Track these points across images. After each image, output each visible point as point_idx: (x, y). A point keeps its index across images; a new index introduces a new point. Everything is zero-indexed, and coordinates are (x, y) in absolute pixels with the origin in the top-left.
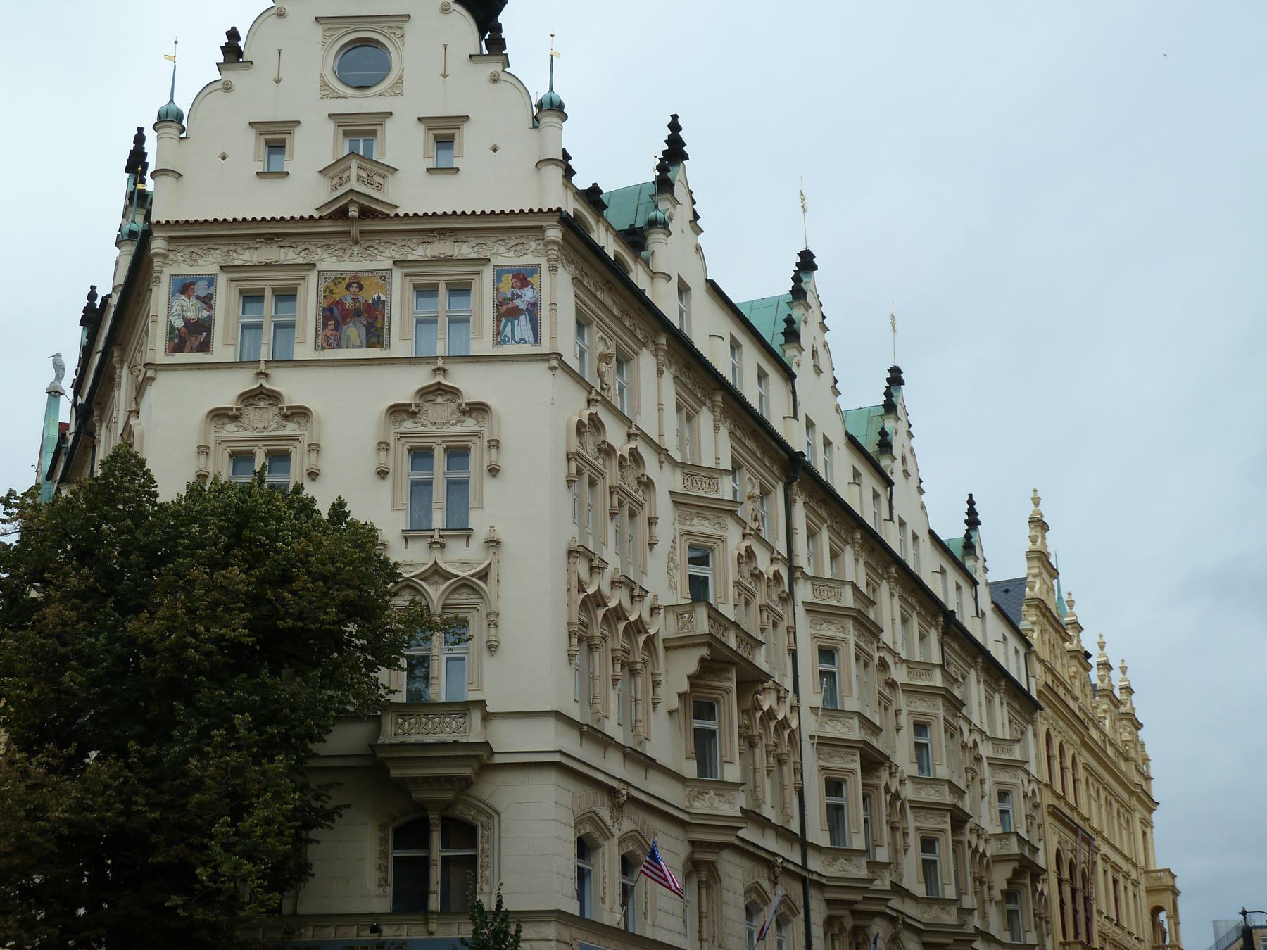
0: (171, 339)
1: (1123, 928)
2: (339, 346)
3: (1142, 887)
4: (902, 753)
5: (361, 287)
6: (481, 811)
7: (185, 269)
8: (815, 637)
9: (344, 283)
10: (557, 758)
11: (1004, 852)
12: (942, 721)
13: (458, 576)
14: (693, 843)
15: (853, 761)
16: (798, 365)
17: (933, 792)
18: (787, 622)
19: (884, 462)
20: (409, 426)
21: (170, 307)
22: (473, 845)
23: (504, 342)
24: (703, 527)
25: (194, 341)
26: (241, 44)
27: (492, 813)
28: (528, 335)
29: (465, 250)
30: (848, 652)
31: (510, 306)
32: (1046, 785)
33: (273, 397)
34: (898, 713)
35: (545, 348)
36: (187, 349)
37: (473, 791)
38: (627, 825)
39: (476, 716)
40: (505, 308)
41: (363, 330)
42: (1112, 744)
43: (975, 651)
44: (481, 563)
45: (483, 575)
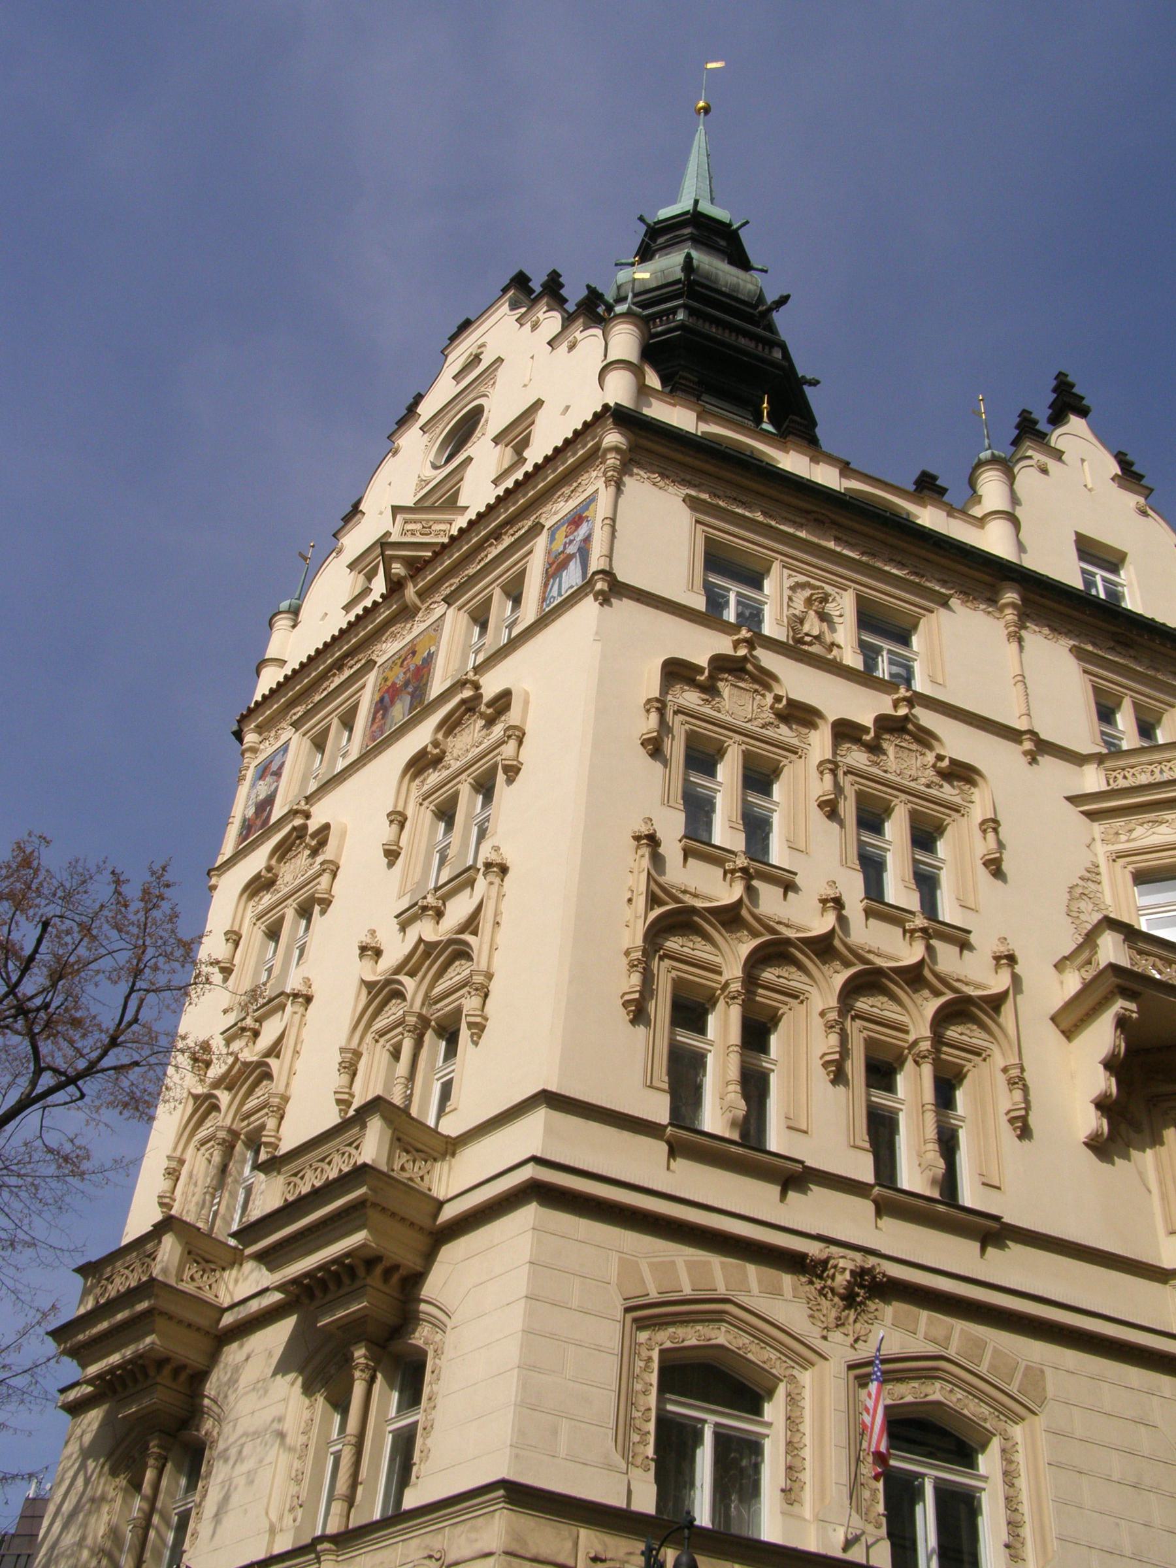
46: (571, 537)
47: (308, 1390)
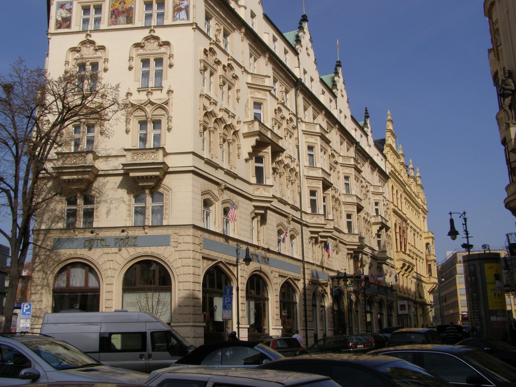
0: (57, 24)
1: (417, 249)
2: (116, 24)
3: (423, 237)
4: (338, 183)
5: (125, 3)
6: (165, 189)
8: (306, 142)
10: (193, 169)
11: (377, 221)
12: (354, 176)
13: (157, 104)
14: (254, 206)
15: (319, 184)
16: (301, 51)
17: (350, 199)
18: (295, 136)
19: (334, 91)
20: (141, 51)
21: (57, 13)
22: (163, 201)
23: (176, 20)
25: (65, 25)
27: (168, 189)
30: (318, 147)
31: (179, 7)
32: (391, 202)
33: (92, 43)
34: (338, 172)
35: (191, 21)
39: (161, 152)
40: (177, 8)
41: (125, 18)
42: (414, 193)
43: (366, 157)
45: (167, 103)
47: (128, 193)
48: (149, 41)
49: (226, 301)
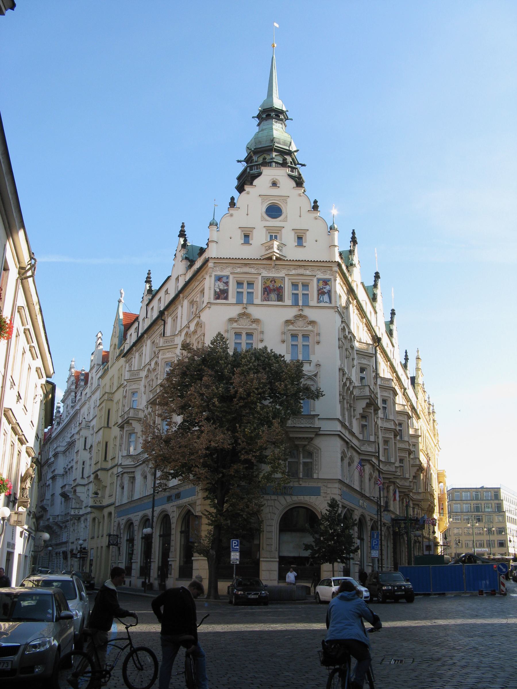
5: (275, 282)
7: (219, 273)
9: (270, 280)
10: (339, 433)
20: (291, 327)
21: (215, 285)
23: (321, 302)
24: (364, 361)
26: (235, 201)
27: (319, 449)
28: (328, 300)
29: (308, 272)
30: (391, 401)
35: (333, 305)
36: (220, 298)
37: (312, 442)
38: (350, 454)
40: (320, 292)
44: (314, 371)
45: (315, 375)
46: (325, 287)
48: (297, 318)
49: (374, 543)
